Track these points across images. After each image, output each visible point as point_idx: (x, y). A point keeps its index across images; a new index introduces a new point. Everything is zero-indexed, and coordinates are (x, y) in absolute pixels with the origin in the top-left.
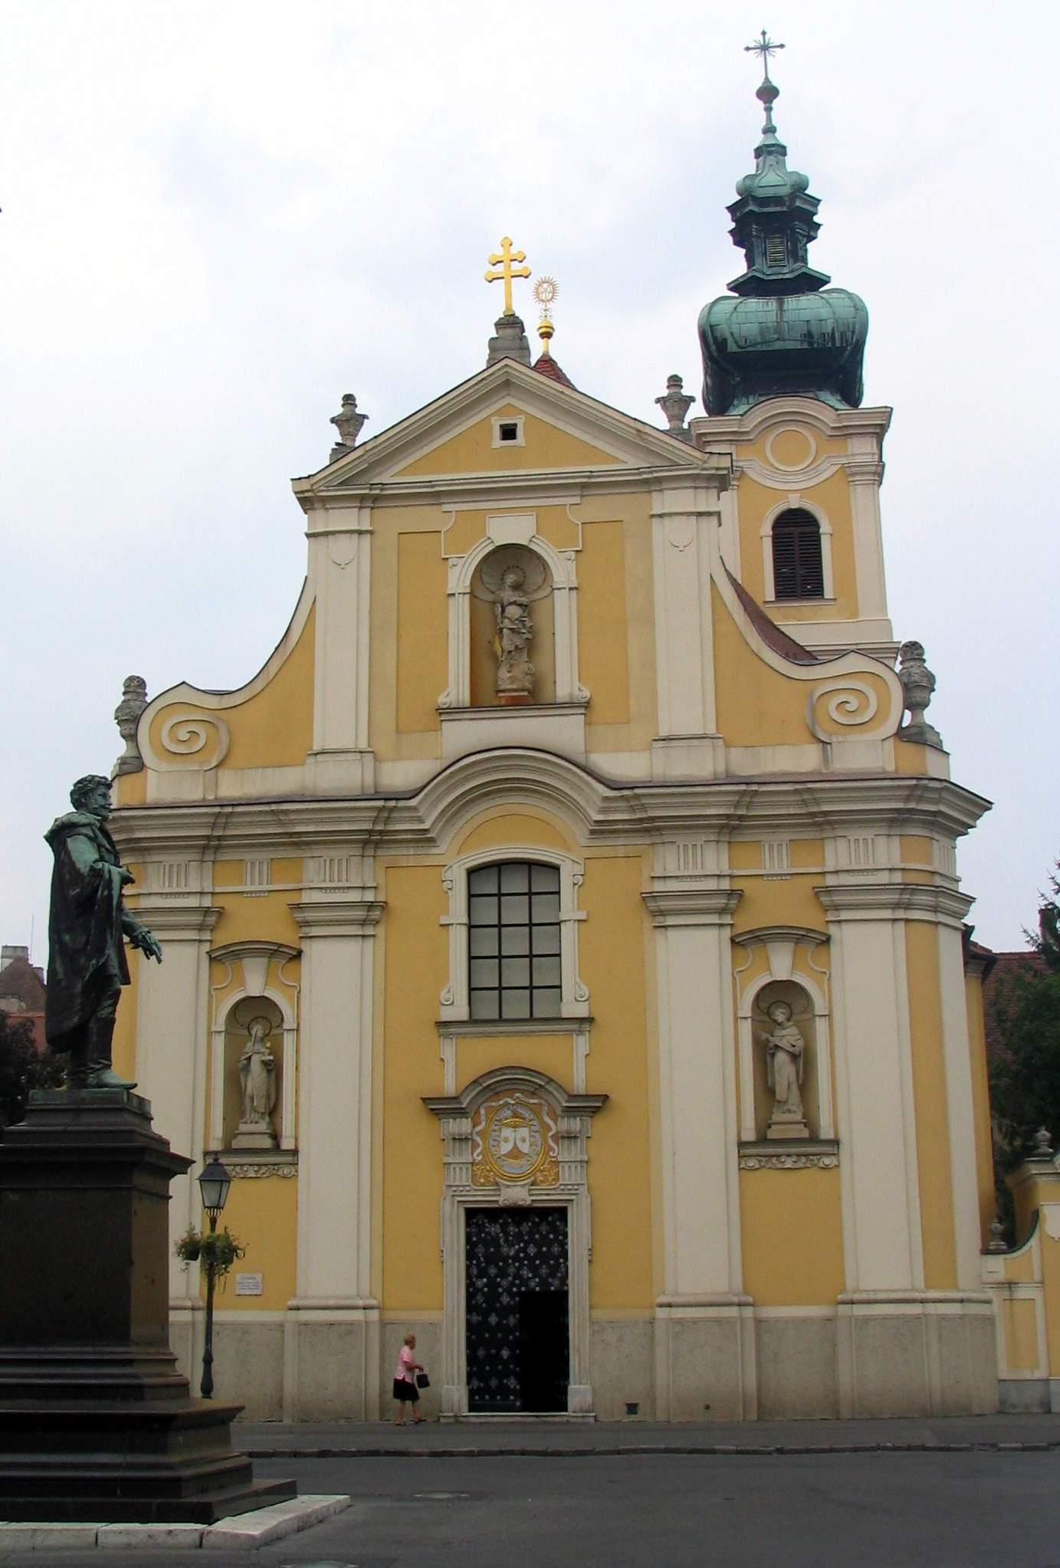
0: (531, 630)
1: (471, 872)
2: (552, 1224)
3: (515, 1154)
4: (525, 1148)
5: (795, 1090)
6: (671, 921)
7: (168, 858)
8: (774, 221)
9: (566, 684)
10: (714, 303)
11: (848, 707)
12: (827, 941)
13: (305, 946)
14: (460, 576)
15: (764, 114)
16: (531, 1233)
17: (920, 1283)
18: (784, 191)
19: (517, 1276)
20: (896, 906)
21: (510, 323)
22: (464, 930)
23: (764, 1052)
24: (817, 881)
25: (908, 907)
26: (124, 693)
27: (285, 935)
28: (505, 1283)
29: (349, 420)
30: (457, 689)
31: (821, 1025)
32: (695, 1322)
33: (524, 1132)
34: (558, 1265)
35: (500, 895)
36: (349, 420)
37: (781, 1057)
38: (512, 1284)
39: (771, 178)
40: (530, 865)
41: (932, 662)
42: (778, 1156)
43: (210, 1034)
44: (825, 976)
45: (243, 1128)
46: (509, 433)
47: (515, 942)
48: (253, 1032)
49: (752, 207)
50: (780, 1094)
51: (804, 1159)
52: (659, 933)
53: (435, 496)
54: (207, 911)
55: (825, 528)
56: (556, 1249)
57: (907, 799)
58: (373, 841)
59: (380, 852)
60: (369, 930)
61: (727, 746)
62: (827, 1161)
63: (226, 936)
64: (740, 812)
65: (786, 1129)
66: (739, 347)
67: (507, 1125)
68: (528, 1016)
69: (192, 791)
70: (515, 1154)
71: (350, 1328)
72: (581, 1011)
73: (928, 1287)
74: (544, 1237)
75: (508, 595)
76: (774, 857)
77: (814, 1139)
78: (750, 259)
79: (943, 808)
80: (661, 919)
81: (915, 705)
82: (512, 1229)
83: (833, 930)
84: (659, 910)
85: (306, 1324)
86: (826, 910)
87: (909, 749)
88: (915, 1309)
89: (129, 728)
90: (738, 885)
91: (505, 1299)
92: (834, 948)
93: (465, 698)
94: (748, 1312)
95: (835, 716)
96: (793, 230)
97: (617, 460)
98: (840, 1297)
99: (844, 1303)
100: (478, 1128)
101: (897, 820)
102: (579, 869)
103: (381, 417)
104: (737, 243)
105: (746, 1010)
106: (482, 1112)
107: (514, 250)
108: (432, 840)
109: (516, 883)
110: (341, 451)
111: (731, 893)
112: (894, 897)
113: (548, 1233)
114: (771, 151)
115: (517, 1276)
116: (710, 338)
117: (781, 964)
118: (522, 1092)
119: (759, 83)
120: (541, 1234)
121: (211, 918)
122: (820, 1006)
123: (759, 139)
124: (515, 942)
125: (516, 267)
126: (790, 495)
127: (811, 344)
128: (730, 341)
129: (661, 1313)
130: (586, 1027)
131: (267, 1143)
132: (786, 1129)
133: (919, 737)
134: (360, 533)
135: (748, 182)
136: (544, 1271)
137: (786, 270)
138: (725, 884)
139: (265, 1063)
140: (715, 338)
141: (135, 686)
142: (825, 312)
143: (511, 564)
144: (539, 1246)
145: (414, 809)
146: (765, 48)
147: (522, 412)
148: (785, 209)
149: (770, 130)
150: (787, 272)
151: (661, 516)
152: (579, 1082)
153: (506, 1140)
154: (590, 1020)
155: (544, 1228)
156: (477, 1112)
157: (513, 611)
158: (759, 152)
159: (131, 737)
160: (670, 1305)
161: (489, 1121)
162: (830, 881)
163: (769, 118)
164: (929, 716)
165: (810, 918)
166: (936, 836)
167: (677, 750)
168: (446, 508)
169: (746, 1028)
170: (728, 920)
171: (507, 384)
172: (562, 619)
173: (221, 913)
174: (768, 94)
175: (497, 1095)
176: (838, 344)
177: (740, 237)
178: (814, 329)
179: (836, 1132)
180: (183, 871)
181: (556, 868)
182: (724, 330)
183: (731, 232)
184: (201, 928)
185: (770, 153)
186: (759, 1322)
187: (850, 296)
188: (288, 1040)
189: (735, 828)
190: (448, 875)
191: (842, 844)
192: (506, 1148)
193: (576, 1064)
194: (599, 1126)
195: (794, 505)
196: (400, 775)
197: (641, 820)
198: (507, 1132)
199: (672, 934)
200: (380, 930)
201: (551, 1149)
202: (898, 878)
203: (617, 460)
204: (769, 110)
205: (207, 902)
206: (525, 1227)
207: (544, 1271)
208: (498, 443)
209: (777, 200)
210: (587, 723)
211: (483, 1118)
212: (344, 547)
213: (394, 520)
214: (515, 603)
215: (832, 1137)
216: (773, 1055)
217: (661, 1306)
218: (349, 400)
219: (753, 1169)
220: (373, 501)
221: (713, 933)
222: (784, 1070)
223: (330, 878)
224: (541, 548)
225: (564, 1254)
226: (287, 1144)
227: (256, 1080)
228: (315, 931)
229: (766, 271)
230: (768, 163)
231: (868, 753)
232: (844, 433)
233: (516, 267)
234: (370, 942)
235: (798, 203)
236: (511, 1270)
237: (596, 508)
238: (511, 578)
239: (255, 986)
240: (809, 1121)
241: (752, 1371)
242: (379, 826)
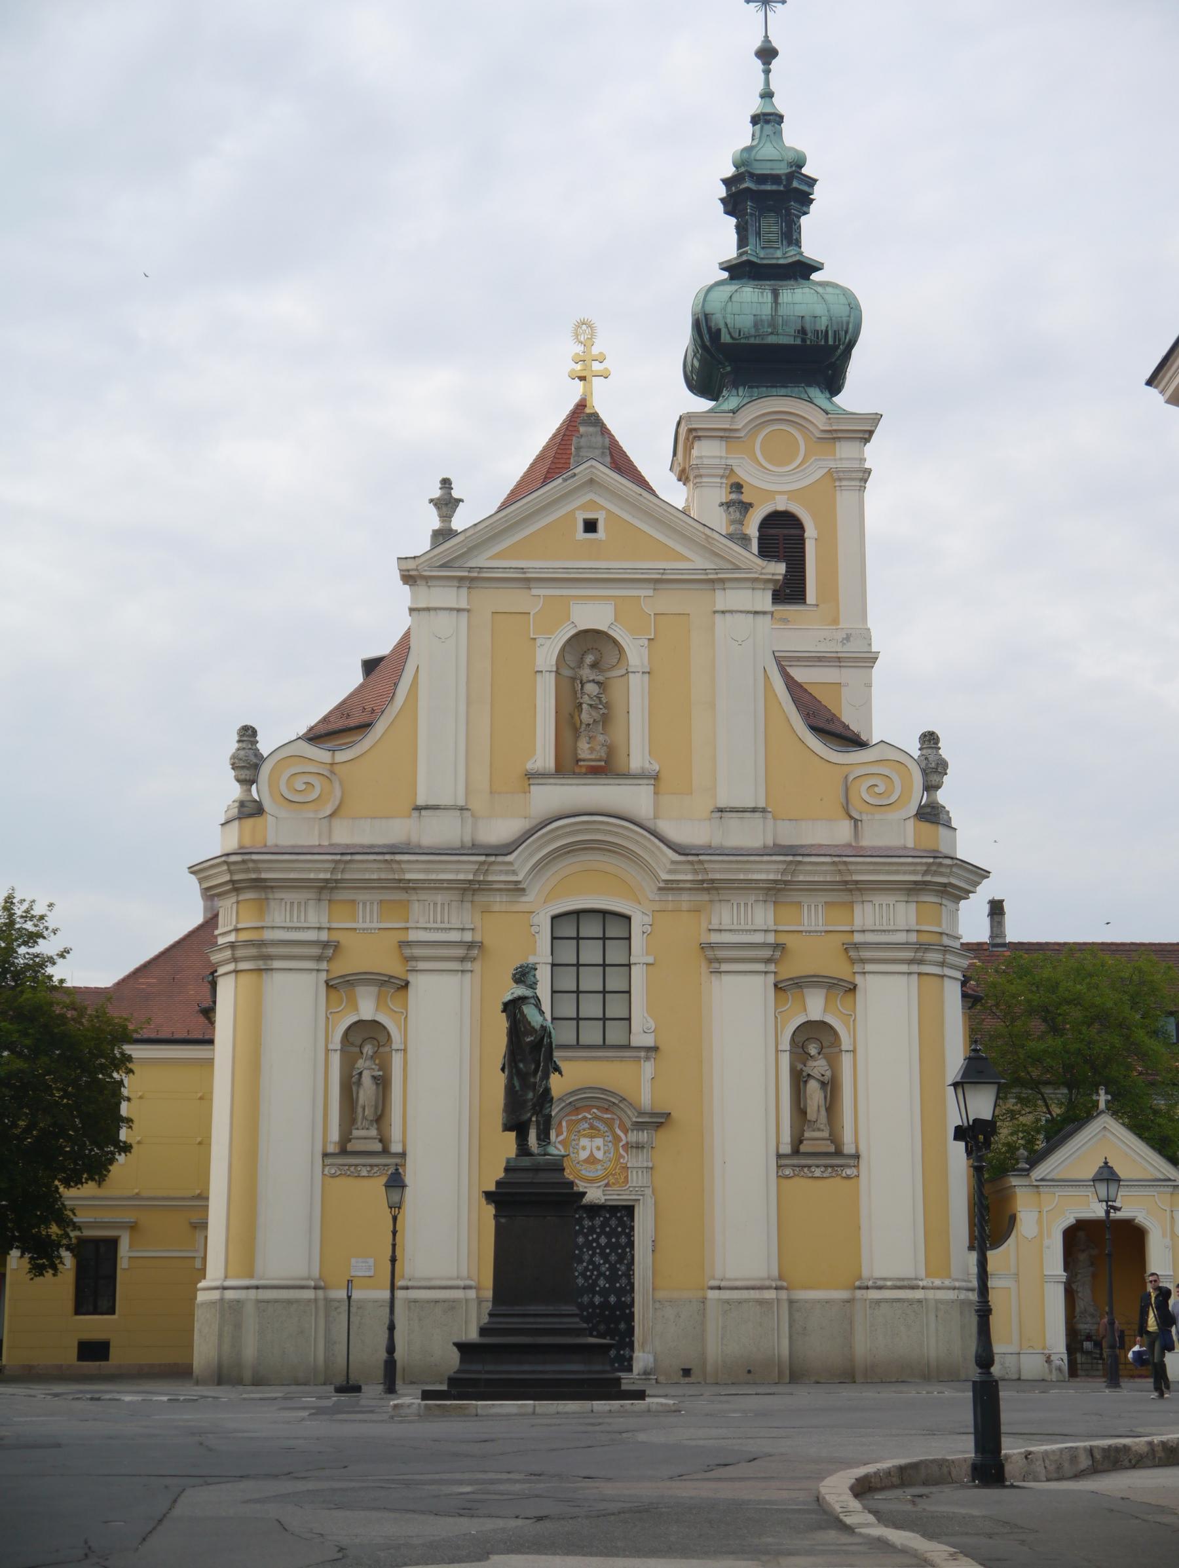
0: (607, 706)
1: (553, 918)
2: (620, 1219)
3: (592, 1160)
4: (599, 1155)
5: (823, 1112)
6: (725, 967)
7: (288, 896)
8: (768, 198)
9: (638, 759)
10: (710, 289)
11: (876, 789)
12: (853, 989)
13: (411, 978)
14: (547, 654)
15: (762, 76)
16: (603, 1226)
17: (922, 1273)
18: (782, 169)
19: (591, 1262)
20: (911, 962)
22: (549, 967)
23: (799, 1080)
24: (846, 938)
25: (921, 962)
26: (239, 741)
27: (393, 967)
28: (580, 1268)
29: (447, 503)
30: (544, 757)
31: (846, 1060)
32: (740, 1302)
33: (599, 1142)
34: (625, 1253)
35: (578, 938)
36: (447, 503)
37: (813, 1085)
38: (586, 1269)
39: (768, 151)
40: (604, 914)
41: (946, 751)
42: (809, 1167)
43: (327, 1051)
44: (850, 1018)
45: (356, 1133)
46: (591, 526)
47: (591, 980)
48: (365, 1051)
49: (748, 184)
50: (811, 1114)
51: (830, 1170)
52: (714, 978)
53: (526, 582)
54: (325, 945)
55: (810, 532)
56: (623, 1240)
57: (925, 873)
58: (470, 890)
59: (476, 898)
60: (468, 966)
61: (775, 819)
62: (849, 1171)
63: (342, 967)
64: (787, 877)
65: (815, 1144)
66: (732, 337)
67: (584, 1136)
68: (601, 1043)
69: (310, 838)
70: (592, 1160)
71: (452, 1305)
72: (649, 1041)
73: (927, 1276)
74: (614, 1230)
75: (586, 673)
76: (813, 916)
77: (838, 1153)
78: (742, 242)
79: (954, 881)
80: (717, 965)
81: (931, 787)
82: (587, 1223)
83: (858, 980)
84: (714, 957)
85: (415, 1301)
86: (853, 962)
87: (925, 827)
88: (918, 1294)
89: (245, 774)
90: (783, 939)
91: (580, 1281)
92: (859, 994)
93: (550, 764)
94: (783, 1295)
96: (788, 210)
97: (689, 560)
98: (857, 1283)
99: (860, 1288)
100: (561, 1138)
101: (914, 889)
102: (648, 920)
104: (727, 212)
105: (785, 1044)
106: (564, 1124)
107: (595, 351)
108: (523, 890)
109: (591, 928)
110: (442, 535)
111: (777, 946)
112: (909, 955)
113: (617, 1226)
114: (767, 120)
115: (591, 1262)
116: (705, 331)
117: (815, 1007)
118: (598, 1108)
119: (758, 43)
120: (610, 1227)
121: (328, 950)
122: (846, 1043)
123: (755, 105)
124: (591, 980)
125: (596, 366)
126: (778, 497)
127: (804, 340)
128: (724, 331)
129: (712, 1295)
130: (653, 1054)
131: (378, 1147)
132: (815, 1144)
133: (931, 814)
134: (458, 610)
135: (745, 155)
136: (613, 1258)
137: (779, 254)
138: (771, 938)
139: (374, 1077)
140: (709, 328)
141: (248, 734)
142: (820, 310)
143: (590, 650)
144: (609, 1236)
145: (510, 863)
147: (603, 508)
148: (782, 188)
149: (767, 95)
150: (782, 255)
151: (723, 612)
152: (646, 1099)
153: (584, 1148)
154: (655, 1049)
155: (613, 1222)
156: (560, 1123)
157: (591, 688)
158: (755, 120)
159: (247, 783)
160: (719, 1288)
161: (569, 1131)
162: (858, 938)
164: (942, 797)
165: (839, 969)
166: (945, 902)
167: (733, 821)
168: (535, 592)
169: (785, 1059)
170: (772, 967)
171: (591, 481)
172: (635, 698)
173: (337, 946)
174: (767, 54)
175: (577, 1110)
176: (831, 342)
177: (732, 204)
178: (808, 327)
179: (857, 1148)
180: (302, 909)
181: (629, 918)
182: (718, 320)
183: (722, 200)
184: (319, 959)
185: (767, 122)
186: (791, 1302)
187: (846, 293)
188: (397, 1060)
189: (779, 890)
190: (536, 920)
191: (868, 907)
192: (584, 1155)
193: (643, 1085)
194: (662, 1138)
195: (781, 507)
196: (500, 829)
197: (703, 881)
198: (584, 1142)
199: (725, 978)
200: (477, 966)
201: (622, 1156)
202: (913, 938)
204: (767, 72)
205: (324, 936)
206: (598, 1221)
207: (613, 1258)
208: (580, 534)
209: (775, 179)
210: (656, 793)
211: (564, 1129)
212: (444, 622)
213: (491, 600)
214: (593, 681)
215: (853, 1151)
216: (806, 1082)
217: (712, 1288)
218: (446, 483)
219: (787, 1177)
220: (470, 581)
221: (760, 979)
222: (814, 1094)
223: (435, 920)
224: (618, 634)
225: (631, 1244)
226: (396, 1148)
227: (367, 1092)
228: (421, 965)
229: (757, 253)
230: (766, 132)
231: (895, 830)
232: (833, 437)
233: (596, 366)
234: (468, 976)
235: (795, 184)
236: (586, 1257)
237: (668, 601)
238: (589, 659)
239: (367, 1009)
240: (835, 1138)
241: (785, 1343)
242: (480, 875)
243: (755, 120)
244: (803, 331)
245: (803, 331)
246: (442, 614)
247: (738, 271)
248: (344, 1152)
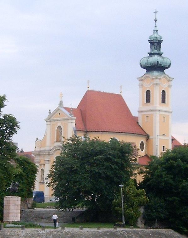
21: (61, 102)
29: (50, 113)
30: (55, 140)
103: (52, 111)
119: (154, 19)
146: (156, 12)
174: (156, 20)
195: (148, 90)
213: (52, 123)
247: (151, 54)
248: (41, 182)
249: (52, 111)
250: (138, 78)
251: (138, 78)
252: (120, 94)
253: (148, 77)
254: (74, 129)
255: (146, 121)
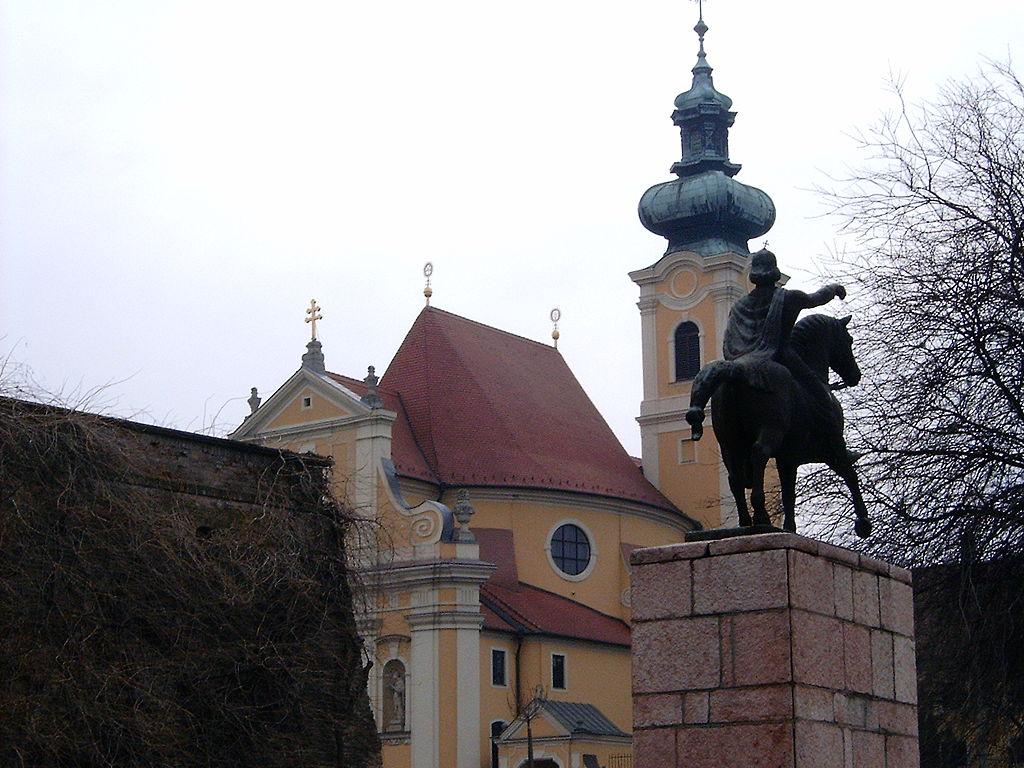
8: (704, 120)
11: (424, 528)
12: (410, 640)
20: (434, 623)
21: (315, 347)
25: (440, 623)
29: (254, 401)
46: (308, 402)
87: (448, 547)
95: (421, 534)
97: (347, 413)
101: (435, 582)
103: (265, 396)
107: (316, 305)
114: (702, 72)
123: (694, 61)
126: (683, 314)
142: (702, 191)
149: (702, 55)
163: (702, 46)
174: (701, 29)
203: (347, 413)
204: (702, 40)
208: (303, 408)
235: (702, 112)
243: (695, 71)
244: (694, 207)
245: (694, 207)
246: (365, 441)
249: (265, 396)
250: (630, 274)
251: (630, 274)
252: (551, 343)
253: (684, 264)
254: (385, 467)
255: (680, 460)
